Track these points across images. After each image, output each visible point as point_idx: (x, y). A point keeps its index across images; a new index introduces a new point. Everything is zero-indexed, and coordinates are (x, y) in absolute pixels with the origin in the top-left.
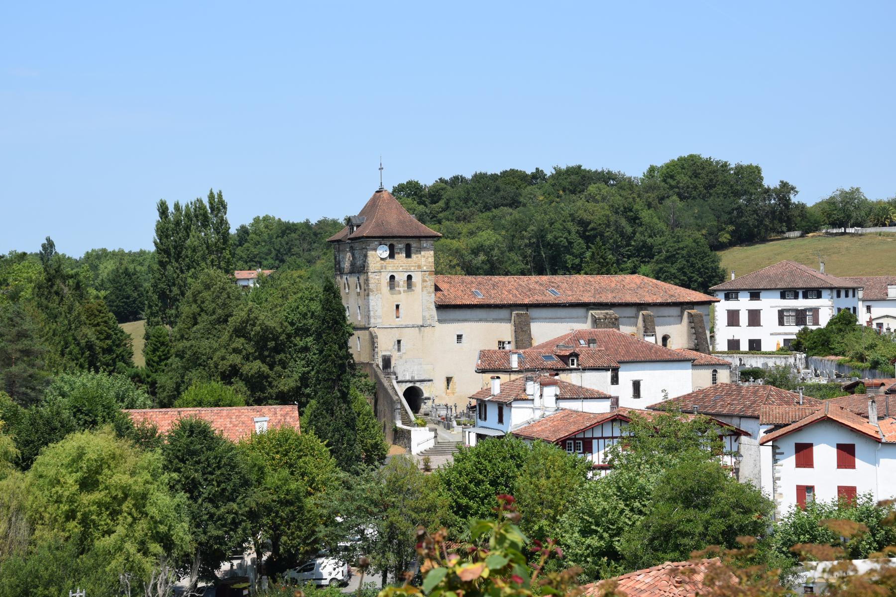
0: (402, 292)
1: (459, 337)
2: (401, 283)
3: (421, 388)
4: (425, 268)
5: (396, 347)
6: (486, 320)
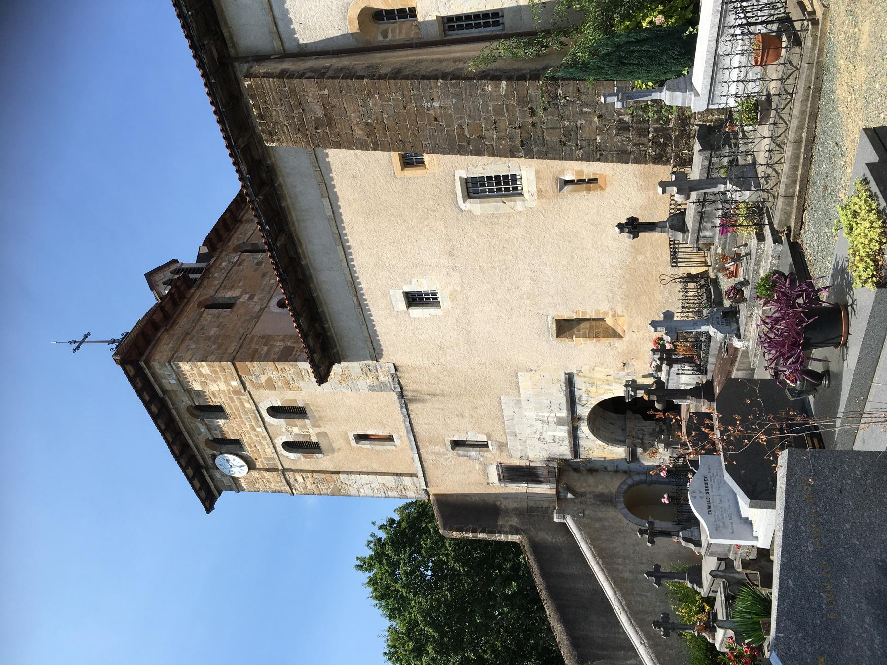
0: (318, 430)
1: (414, 299)
2: (296, 430)
3: (594, 402)
4: (235, 383)
5: (473, 453)
6: (336, 218)
